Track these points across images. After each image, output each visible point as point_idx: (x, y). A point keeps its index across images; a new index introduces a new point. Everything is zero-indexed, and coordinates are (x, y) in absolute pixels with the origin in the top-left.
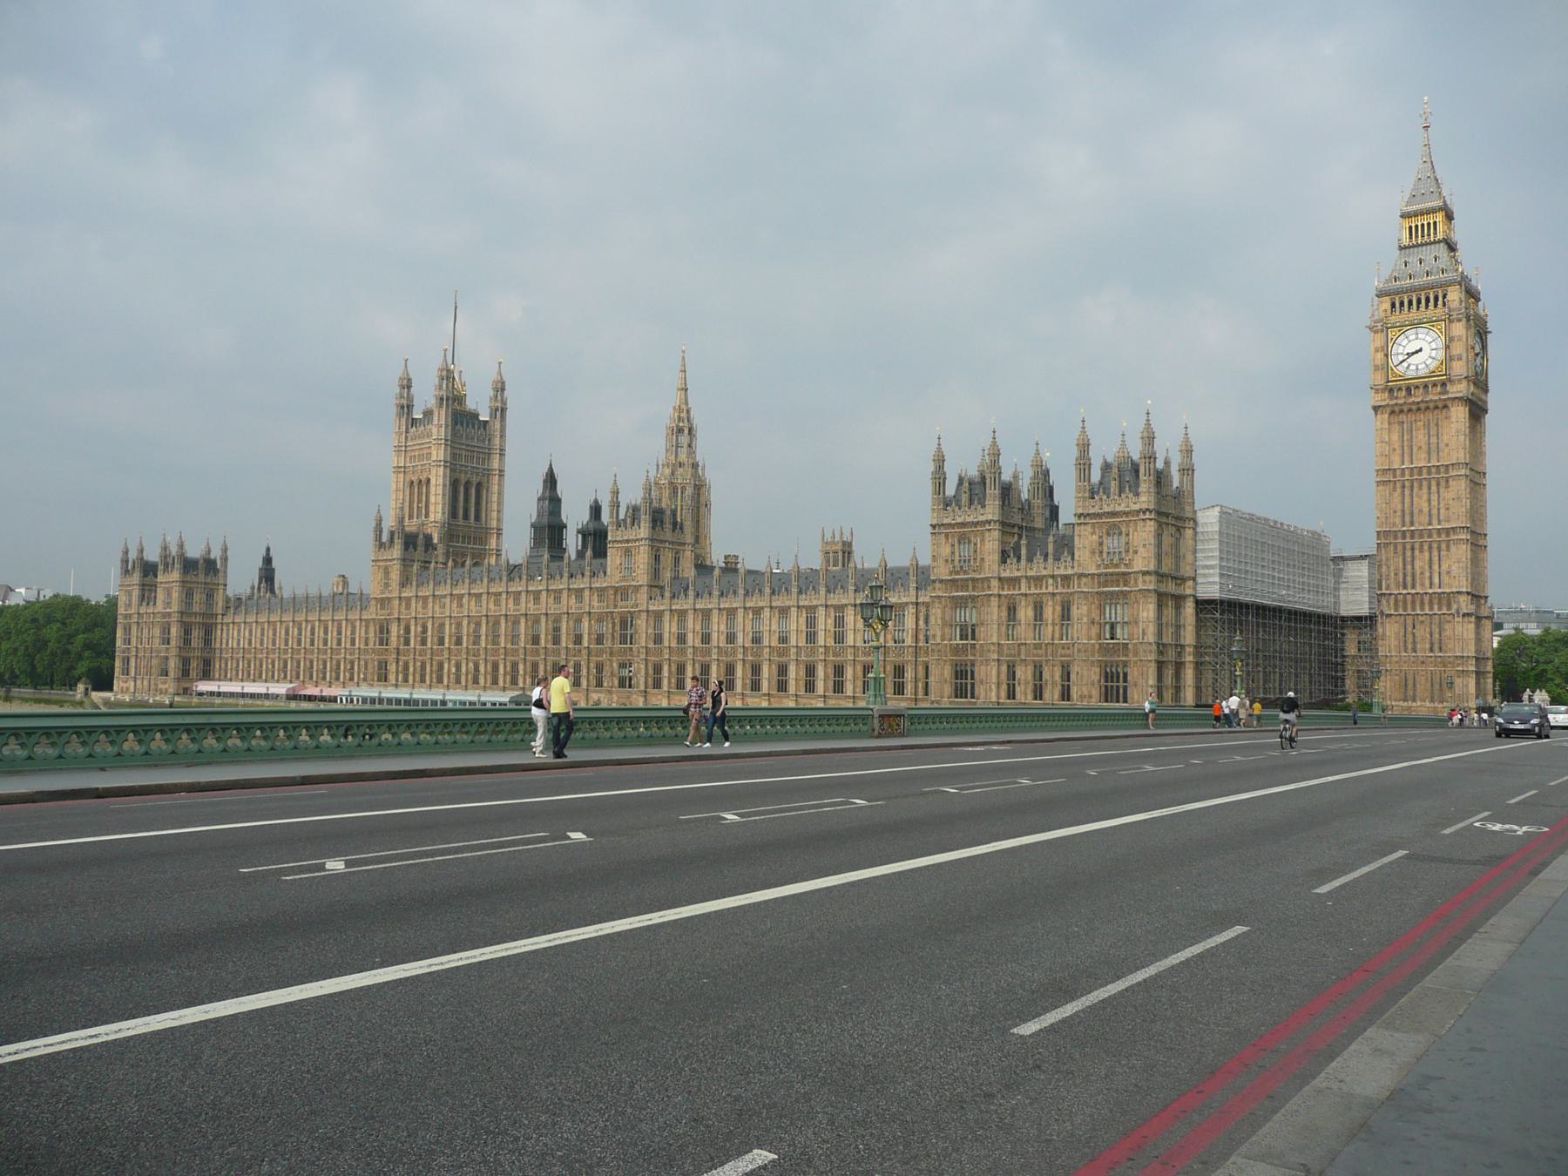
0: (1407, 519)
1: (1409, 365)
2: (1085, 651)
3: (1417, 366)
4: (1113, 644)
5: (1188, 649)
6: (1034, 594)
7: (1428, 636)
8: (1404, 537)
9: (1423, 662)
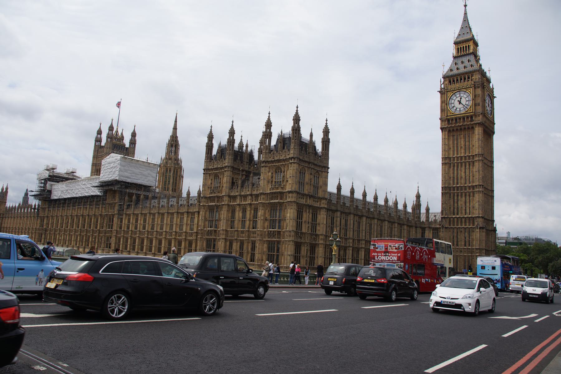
0: (455, 181)
1: (456, 109)
2: (261, 235)
3: (460, 109)
4: (273, 231)
5: (321, 237)
6: (243, 204)
7: (464, 238)
8: (454, 190)
9: (461, 251)
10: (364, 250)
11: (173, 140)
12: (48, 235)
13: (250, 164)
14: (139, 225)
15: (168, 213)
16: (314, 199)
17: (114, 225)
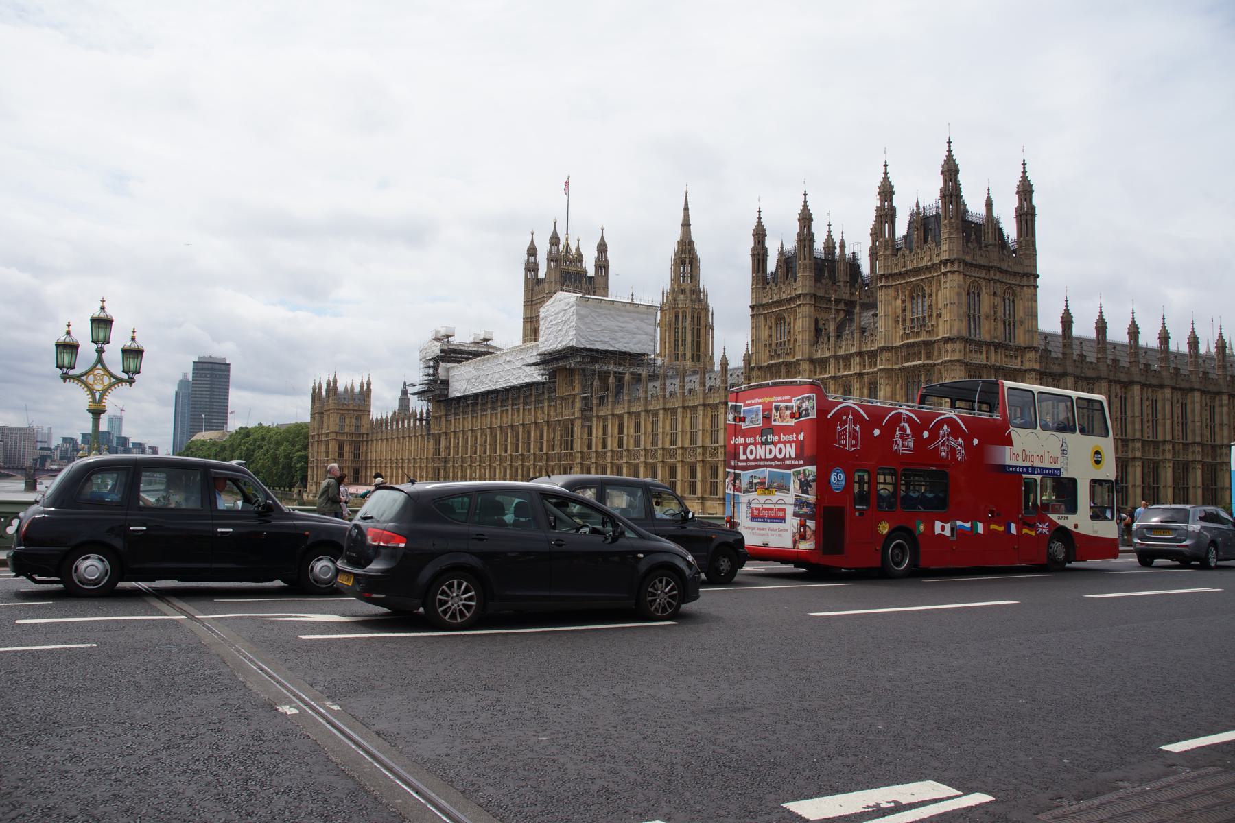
6: (843, 376)
10: (1140, 463)
11: (683, 251)
12: (451, 471)
13: (852, 286)
14: (625, 438)
15: (684, 408)
16: (1008, 352)
17: (575, 441)
